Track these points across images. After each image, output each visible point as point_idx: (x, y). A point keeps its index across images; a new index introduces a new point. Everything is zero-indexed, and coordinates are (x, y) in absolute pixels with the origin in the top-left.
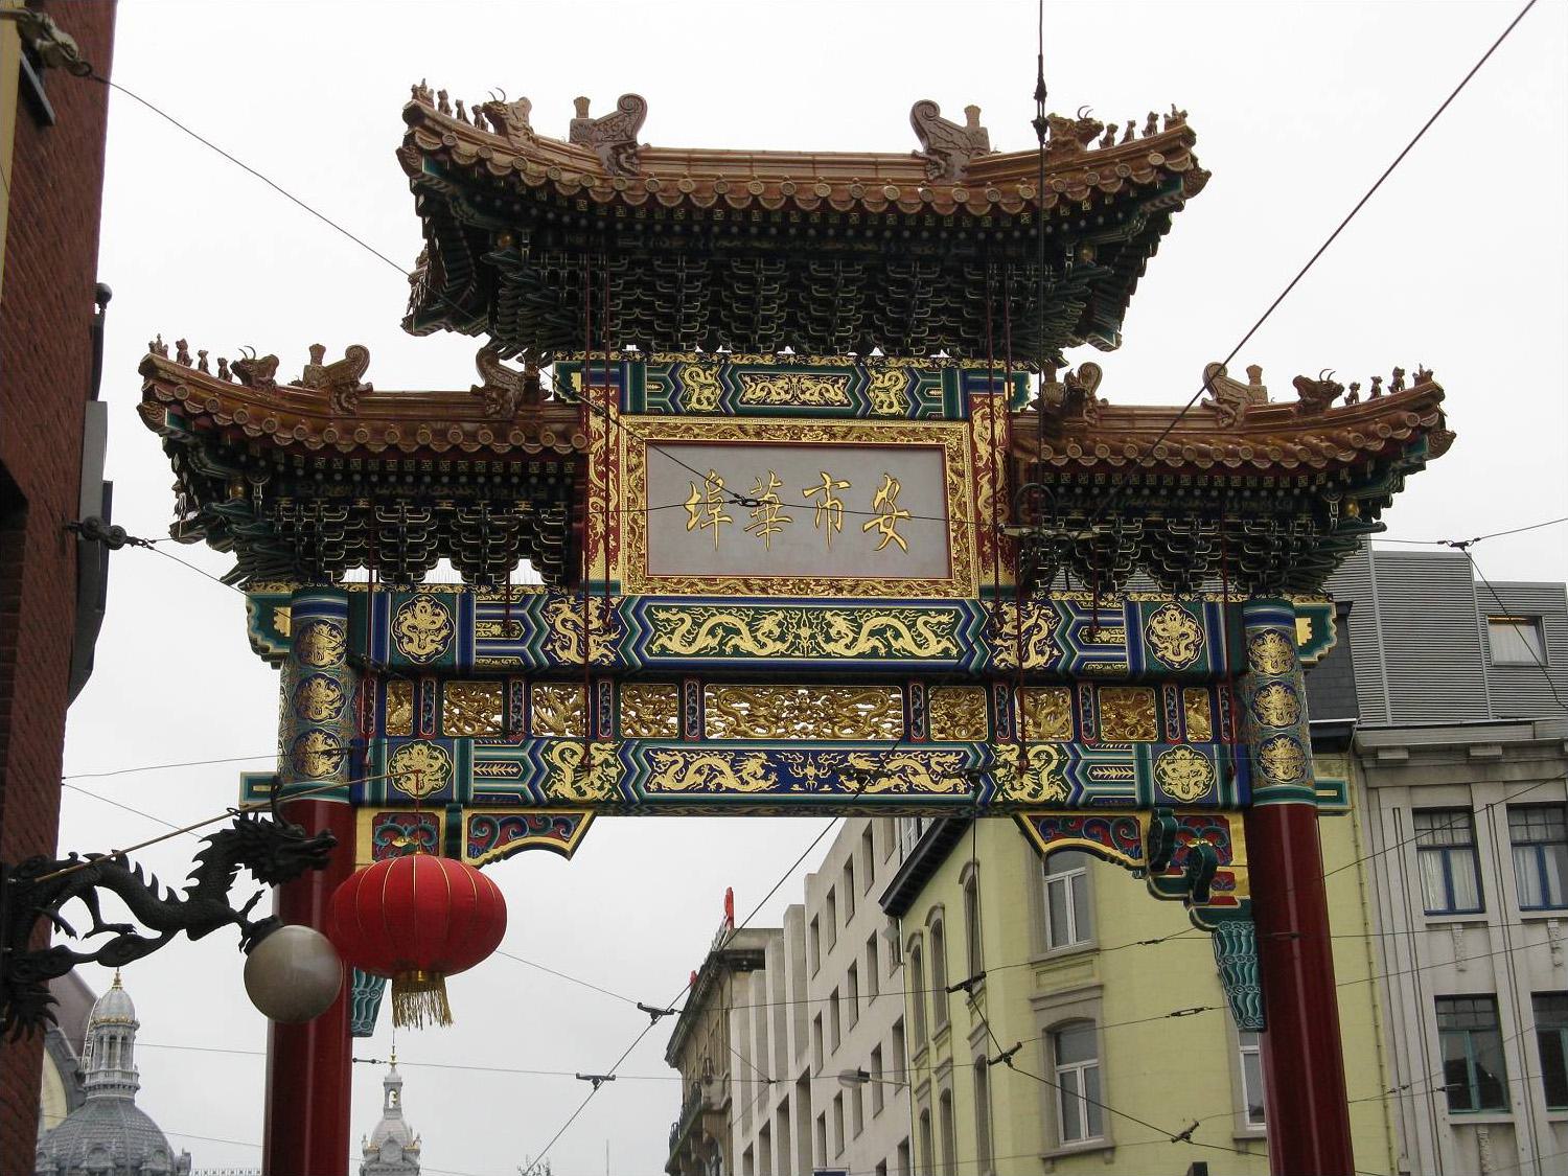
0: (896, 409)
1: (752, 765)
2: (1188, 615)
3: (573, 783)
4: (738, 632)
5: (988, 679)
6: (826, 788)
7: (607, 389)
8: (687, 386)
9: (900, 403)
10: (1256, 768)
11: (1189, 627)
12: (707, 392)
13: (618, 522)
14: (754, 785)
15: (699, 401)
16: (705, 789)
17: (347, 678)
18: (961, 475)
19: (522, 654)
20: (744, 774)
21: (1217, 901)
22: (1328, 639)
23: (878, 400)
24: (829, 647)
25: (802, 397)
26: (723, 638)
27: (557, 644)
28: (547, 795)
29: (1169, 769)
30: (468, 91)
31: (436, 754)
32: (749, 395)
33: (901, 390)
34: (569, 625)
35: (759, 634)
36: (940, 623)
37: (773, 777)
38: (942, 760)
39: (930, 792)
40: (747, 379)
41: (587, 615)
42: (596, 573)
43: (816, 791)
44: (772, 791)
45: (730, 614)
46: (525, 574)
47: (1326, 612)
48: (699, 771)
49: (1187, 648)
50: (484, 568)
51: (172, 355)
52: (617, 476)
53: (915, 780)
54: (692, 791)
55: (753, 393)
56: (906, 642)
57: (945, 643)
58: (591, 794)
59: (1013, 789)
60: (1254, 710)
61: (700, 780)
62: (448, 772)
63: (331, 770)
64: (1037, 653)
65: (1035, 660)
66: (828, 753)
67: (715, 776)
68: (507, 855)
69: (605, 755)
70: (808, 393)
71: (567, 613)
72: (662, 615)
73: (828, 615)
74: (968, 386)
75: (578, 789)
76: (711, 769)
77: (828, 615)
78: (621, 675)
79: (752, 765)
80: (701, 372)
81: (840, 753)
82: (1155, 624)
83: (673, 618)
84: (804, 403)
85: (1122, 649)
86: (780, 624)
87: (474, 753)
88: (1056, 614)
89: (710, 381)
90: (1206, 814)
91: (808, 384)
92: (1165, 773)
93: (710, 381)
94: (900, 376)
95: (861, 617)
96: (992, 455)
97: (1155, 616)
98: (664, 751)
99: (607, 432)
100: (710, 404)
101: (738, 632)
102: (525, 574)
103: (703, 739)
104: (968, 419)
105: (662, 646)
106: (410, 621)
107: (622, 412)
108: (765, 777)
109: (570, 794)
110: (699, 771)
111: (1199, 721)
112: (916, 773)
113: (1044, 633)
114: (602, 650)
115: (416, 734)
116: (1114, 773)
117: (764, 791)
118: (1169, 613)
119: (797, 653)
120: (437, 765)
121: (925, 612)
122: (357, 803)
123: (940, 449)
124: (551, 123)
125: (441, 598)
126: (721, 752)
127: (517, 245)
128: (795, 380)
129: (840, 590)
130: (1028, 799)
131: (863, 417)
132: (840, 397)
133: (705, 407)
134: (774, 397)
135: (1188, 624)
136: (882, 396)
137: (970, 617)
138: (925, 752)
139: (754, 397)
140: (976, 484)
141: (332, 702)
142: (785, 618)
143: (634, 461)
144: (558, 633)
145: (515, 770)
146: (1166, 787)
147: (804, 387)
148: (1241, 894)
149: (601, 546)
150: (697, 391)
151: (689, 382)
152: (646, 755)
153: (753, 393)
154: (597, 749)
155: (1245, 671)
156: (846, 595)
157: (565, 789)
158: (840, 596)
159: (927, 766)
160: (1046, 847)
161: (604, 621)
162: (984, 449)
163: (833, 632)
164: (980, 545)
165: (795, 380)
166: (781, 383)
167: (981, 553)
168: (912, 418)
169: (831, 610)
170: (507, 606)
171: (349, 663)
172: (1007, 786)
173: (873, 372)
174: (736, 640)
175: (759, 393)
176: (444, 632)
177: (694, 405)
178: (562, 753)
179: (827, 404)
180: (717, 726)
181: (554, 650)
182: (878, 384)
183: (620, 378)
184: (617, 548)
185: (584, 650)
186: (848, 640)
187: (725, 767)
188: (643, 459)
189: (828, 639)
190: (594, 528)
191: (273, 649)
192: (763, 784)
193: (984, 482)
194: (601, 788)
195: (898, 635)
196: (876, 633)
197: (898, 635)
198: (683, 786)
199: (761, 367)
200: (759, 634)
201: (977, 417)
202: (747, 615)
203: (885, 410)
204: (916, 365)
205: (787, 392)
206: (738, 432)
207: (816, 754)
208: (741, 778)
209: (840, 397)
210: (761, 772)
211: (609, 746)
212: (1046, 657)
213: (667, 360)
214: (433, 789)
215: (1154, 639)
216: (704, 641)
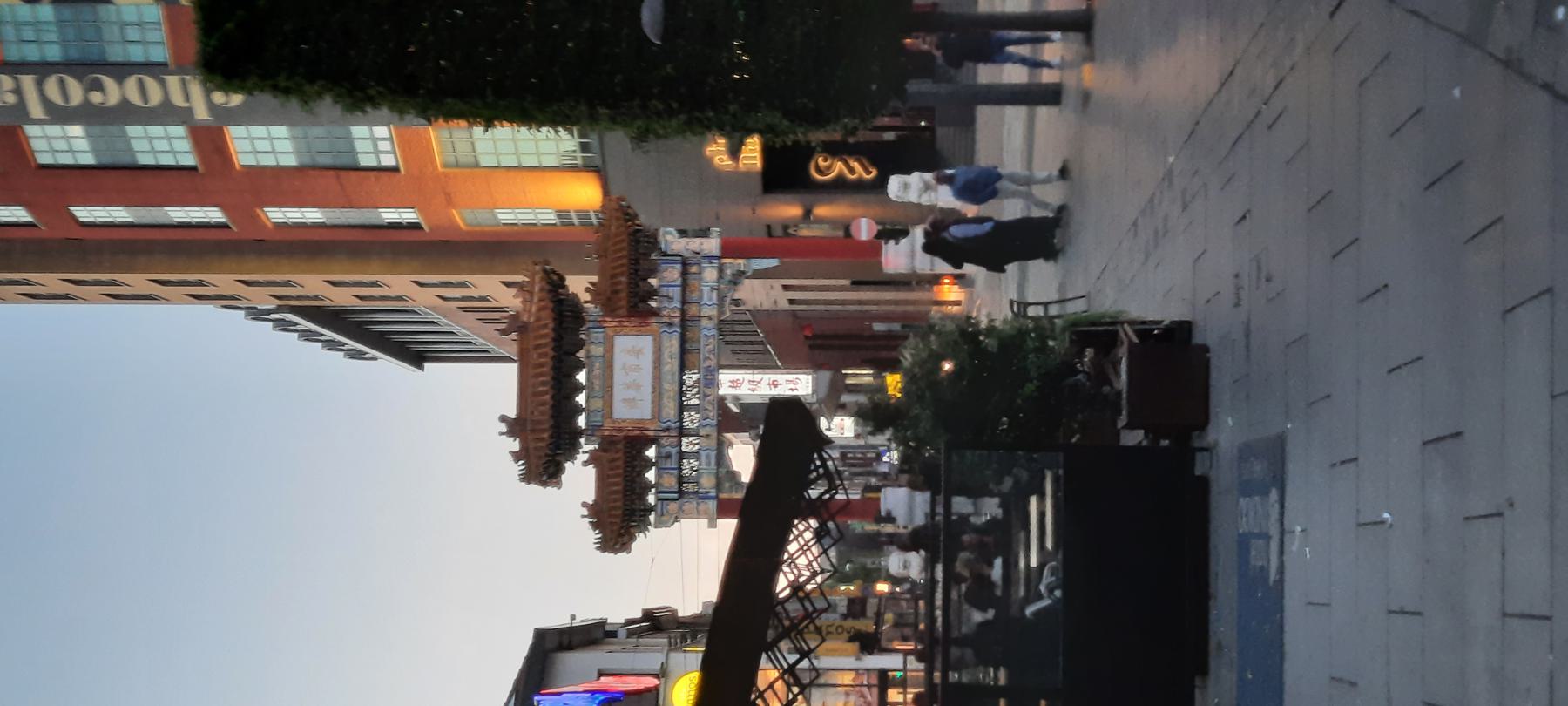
5: (684, 327)
30: (516, 469)
42: (651, 433)
50: (648, 464)
51: (599, 545)
90: (721, 270)
102: (651, 453)
124: (515, 445)
125: (659, 475)
148: (741, 261)
153: (597, 388)
155: (680, 256)
162: (614, 324)
171: (677, 500)
180: (694, 401)
196: (671, 357)
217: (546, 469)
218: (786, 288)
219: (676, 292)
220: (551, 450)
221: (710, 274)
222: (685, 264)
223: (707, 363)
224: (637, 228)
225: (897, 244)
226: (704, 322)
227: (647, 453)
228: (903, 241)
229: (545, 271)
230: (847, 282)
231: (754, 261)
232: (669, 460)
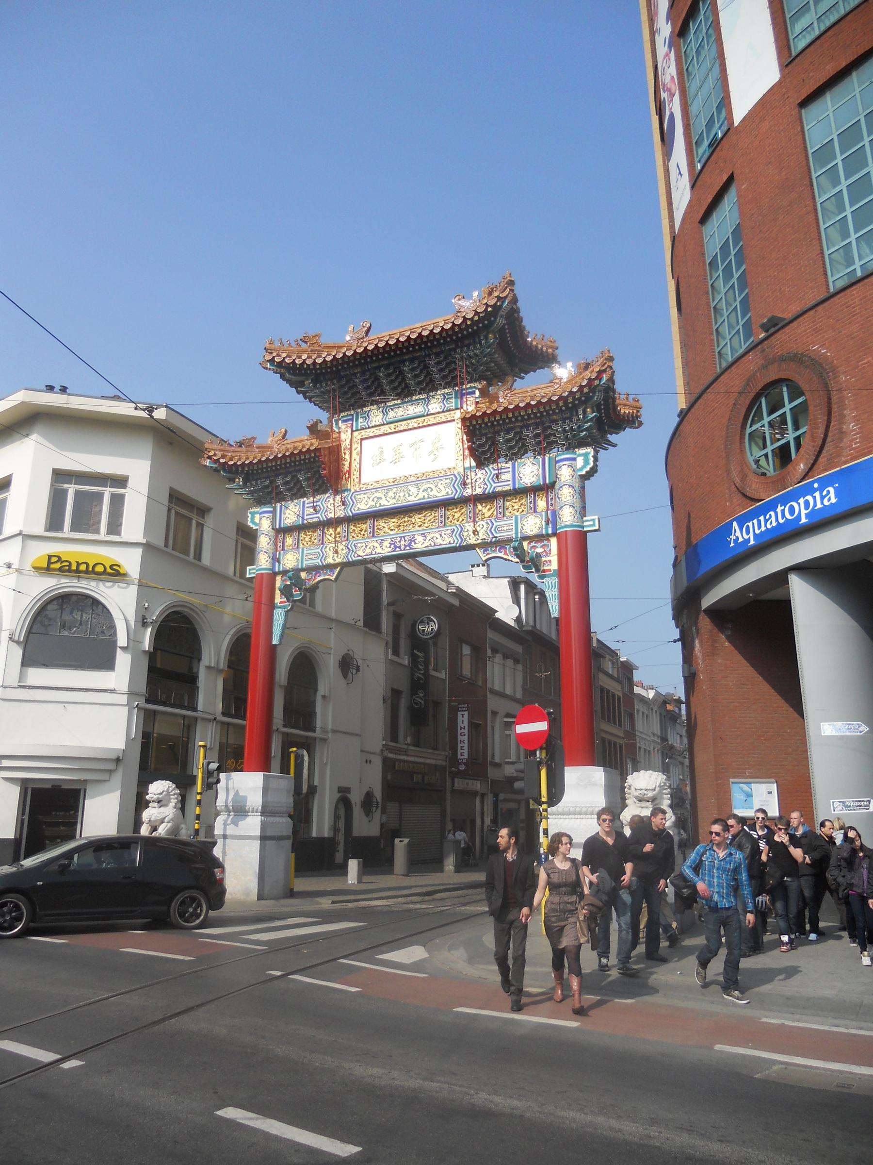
1: (386, 543)
4: (381, 498)
6: (408, 548)
11: (535, 468)
16: (371, 554)
17: (272, 533)
19: (318, 517)
22: (589, 464)
24: (409, 499)
37: (392, 546)
39: (441, 545)
47: (588, 453)
53: (437, 541)
56: (434, 493)
57: (447, 490)
61: (370, 551)
65: (479, 491)
72: (359, 497)
73: (409, 487)
75: (334, 560)
77: (409, 487)
79: (386, 543)
87: (305, 552)
90: (540, 538)
101: (381, 498)
105: (359, 509)
109: (332, 562)
113: (482, 480)
114: (341, 512)
116: (505, 528)
121: (441, 480)
122: (275, 574)
130: (475, 542)
131: (427, 415)
133: (378, 423)
134: (399, 414)
148: (554, 566)
159: (441, 535)
160: (484, 559)
163: (411, 494)
166: (401, 409)
168: (443, 412)
170: (314, 502)
171: (273, 529)
172: (468, 539)
174: (381, 501)
175: (394, 415)
186: (415, 495)
187: (377, 545)
189: (409, 495)
192: (390, 550)
195: (432, 490)
197: (432, 490)
199: (397, 404)
200: (388, 498)
207: (404, 537)
210: (389, 545)
215: (521, 475)
216: (371, 503)
219: (506, 483)
221: (533, 525)
222: (547, 488)
223: (419, 538)
224: (580, 412)
226: (469, 527)
231: (555, 580)
232: (312, 510)
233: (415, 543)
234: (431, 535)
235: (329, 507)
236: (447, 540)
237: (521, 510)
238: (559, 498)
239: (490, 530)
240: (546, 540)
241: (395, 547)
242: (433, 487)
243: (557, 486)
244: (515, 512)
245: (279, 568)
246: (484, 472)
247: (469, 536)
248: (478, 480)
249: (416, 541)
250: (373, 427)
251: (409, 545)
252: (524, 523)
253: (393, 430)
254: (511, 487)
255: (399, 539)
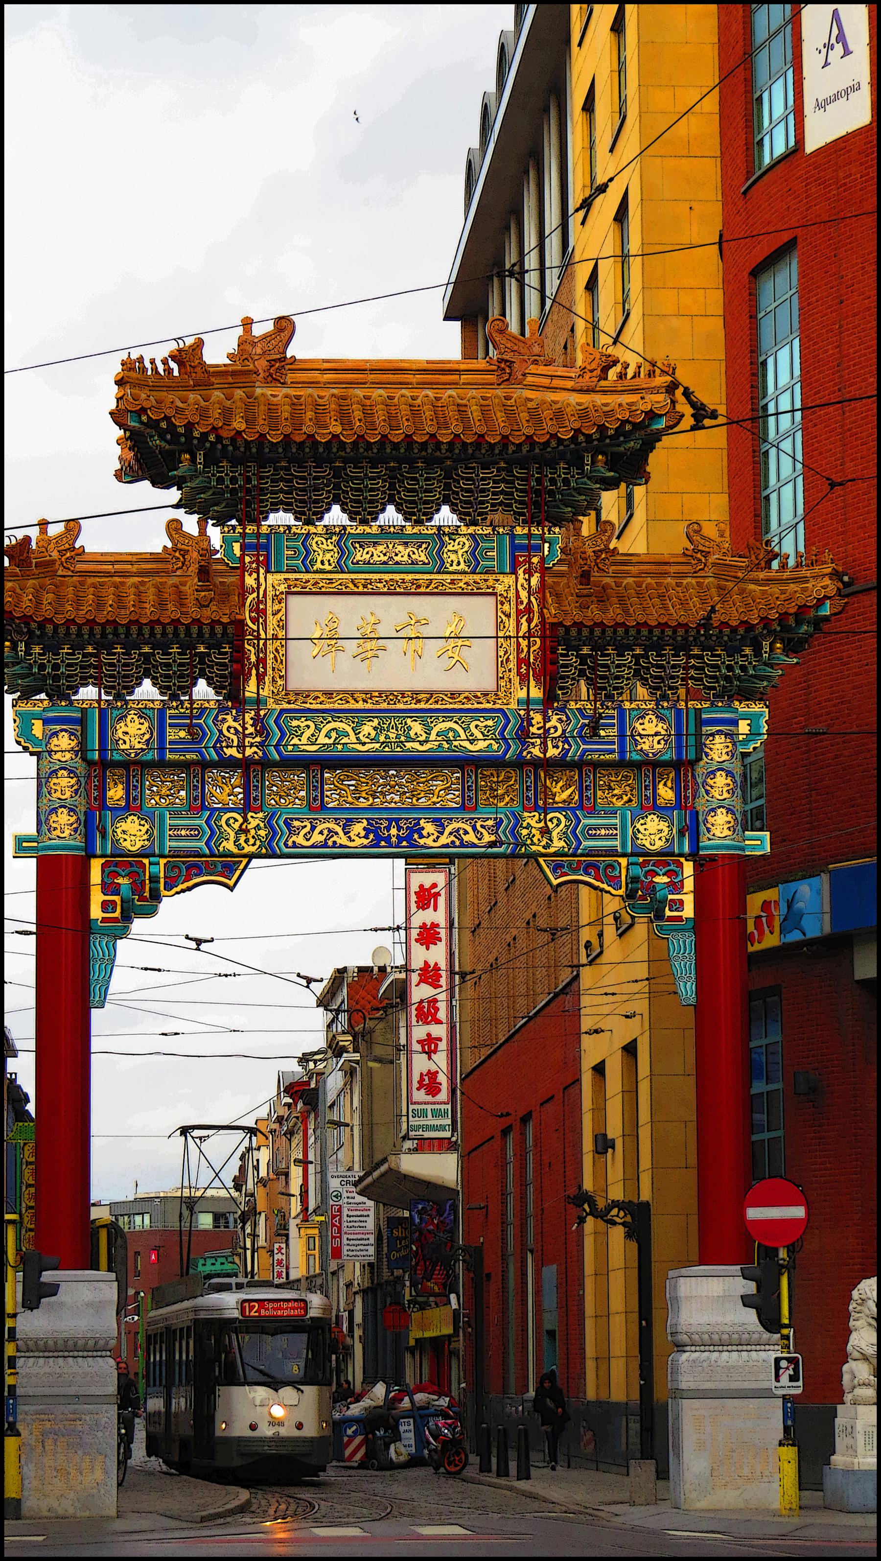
0: (462, 566)
1: (358, 828)
2: (662, 719)
3: (235, 842)
5: (520, 764)
6: (404, 843)
7: (258, 555)
8: (314, 551)
9: (465, 562)
10: (702, 828)
11: (661, 728)
12: (328, 556)
13: (266, 654)
14: (359, 842)
15: (322, 563)
16: (325, 846)
17: (81, 768)
18: (508, 616)
20: (352, 834)
21: (671, 919)
23: (449, 560)
25: (395, 558)
26: (336, 739)
27: (224, 744)
28: (218, 850)
29: (641, 829)
31: (143, 822)
32: (358, 558)
33: (467, 552)
34: (232, 731)
35: (361, 736)
36: (486, 727)
37: (371, 836)
38: (485, 824)
39: (474, 846)
40: (357, 545)
41: (244, 723)
43: (396, 847)
44: (371, 847)
45: (341, 721)
46: (202, 690)
47: (762, 715)
48: (321, 833)
49: (659, 743)
52: (265, 621)
53: (466, 838)
54: (316, 847)
55: (361, 555)
58: (248, 849)
59: (533, 844)
60: (704, 787)
61: (321, 838)
62: (151, 835)
63: (73, 833)
64: (554, 747)
65: (552, 752)
66: (407, 819)
67: (332, 836)
68: (189, 889)
69: (257, 822)
70: (400, 555)
71: (230, 722)
72: (295, 723)
73: (409, 721)
74: (514, 547)
75: (239, 847)
76: (330, 831)
78: (265, 764)
79: (358, 828)
80: (324, 541)
81: (415, 819)
82: (637, 725)
83: (302, 725)
84: (397, 563)
85: (613, 743)
86: (375, 728)
88: (567, 716)
89: (331, 547)
91: (401, 548)
92: (639, 832)
93: (331, 547)
94: (466, 542)
95: (432, 722)
96: (530, 601)
97: (638, 719)
98: (297, 819)
99: (258, 588)
100: (330, 564)
102: (202, 690)
103: (323, 807)
104: (514, 572)
106: (124, 729)
107: (268, 571)
108: (366, 837)
109: (235, 851)
110: (321, 833)
111: (666, 793)
112: (466, 833)
115: (128, 807)
117: (365, 847)
118: (648, 718)
119: (387, 749)
120: (144, 829)
122: (91, 855)
123: (495, 594)
126: (336, 819)
127: (193, 460)
128: (391, 546)
129: (419, 701)
130: (543, 851)
131: (438, 573)
132: (423, 558)
133: (327, 567)
134: (376, 558)
135: (660, 725)
136: (453, 557)
137: (508, 721)
138: (472, 819)
139: (362, 559)
140: (518, 622)
141: (72, 786)
142: (379, 724)
143: (276, 607)
144: (225, 736)
145: (196, 832)
146: (639, 842)
147: (397, 551)
148: (689, 911)
149: (254, 672)
150: (321, 555)
151: (315, 548)
152: (285, 822)
153: (361, 555)
154: (252, 817)
156: (422, 706)
157: (230, 846)
158: (418, 706)
159: (474, 828)
160: (555, 882)
161: (256, 729)
162: (524, 595)
164: (519, 668)
165: (391, 546)
166: (381, 548)
167: (519, 673)
168: (474, 572)
169: (411, 717)
173: (447, 538)
176: (147, 737)
177: (318, 566)
178: (228, 819)
179: (413, 563)
181: (222, 747)
182: (450, 547)
183: (267, 547)
184: (265, 674)
185: (241, 747)
187: (339, 829)
188: (283, 605)
189: (410, 739)
190: (249, 659)
191: (31, 749)
192: (365, 842)
193: (523, 620)
194: (254, 845)
198: (309, 843)
200: (361, 736)
201: (521, 572)
202: (353, 722)
203: (455, 567)
204: (481, 532)
205: (385, 555)
206: (351, 585)
207: (397, 820)
208: (350, 837)
209: (423, 558)
210: (363, 833)
211: (261, 815)
212: (560, 749)
213: (303, 531)
214: (143, 846)
217: (153, 424)
218: (630, 1050)
220: (204, 435)
225: (746, 1300)
227: (202, 683)
228: (750, 1317)
229: (651, 415)
230: (646, 1195)
231: (690, 939)
233: (421, 836)
234: (455, 825)
235: (225, 732)
236: (488, 838)
237: (625, 798)
238: (707, 792)
239: (574, 832)
240: (675, 862)
241: (378, 838)
242: (461, 732)
243: (701, 769)
244: (614, 800)
245: (104, 846)
246: (564, 718)
247: (531, 836)
248: (552, 730)
249: (425, 833)
250: (316, 572)
251: (409, 838)
252: (638, 826)
253: (361, 589)
254: (615, 756)
255: (385, 824)
